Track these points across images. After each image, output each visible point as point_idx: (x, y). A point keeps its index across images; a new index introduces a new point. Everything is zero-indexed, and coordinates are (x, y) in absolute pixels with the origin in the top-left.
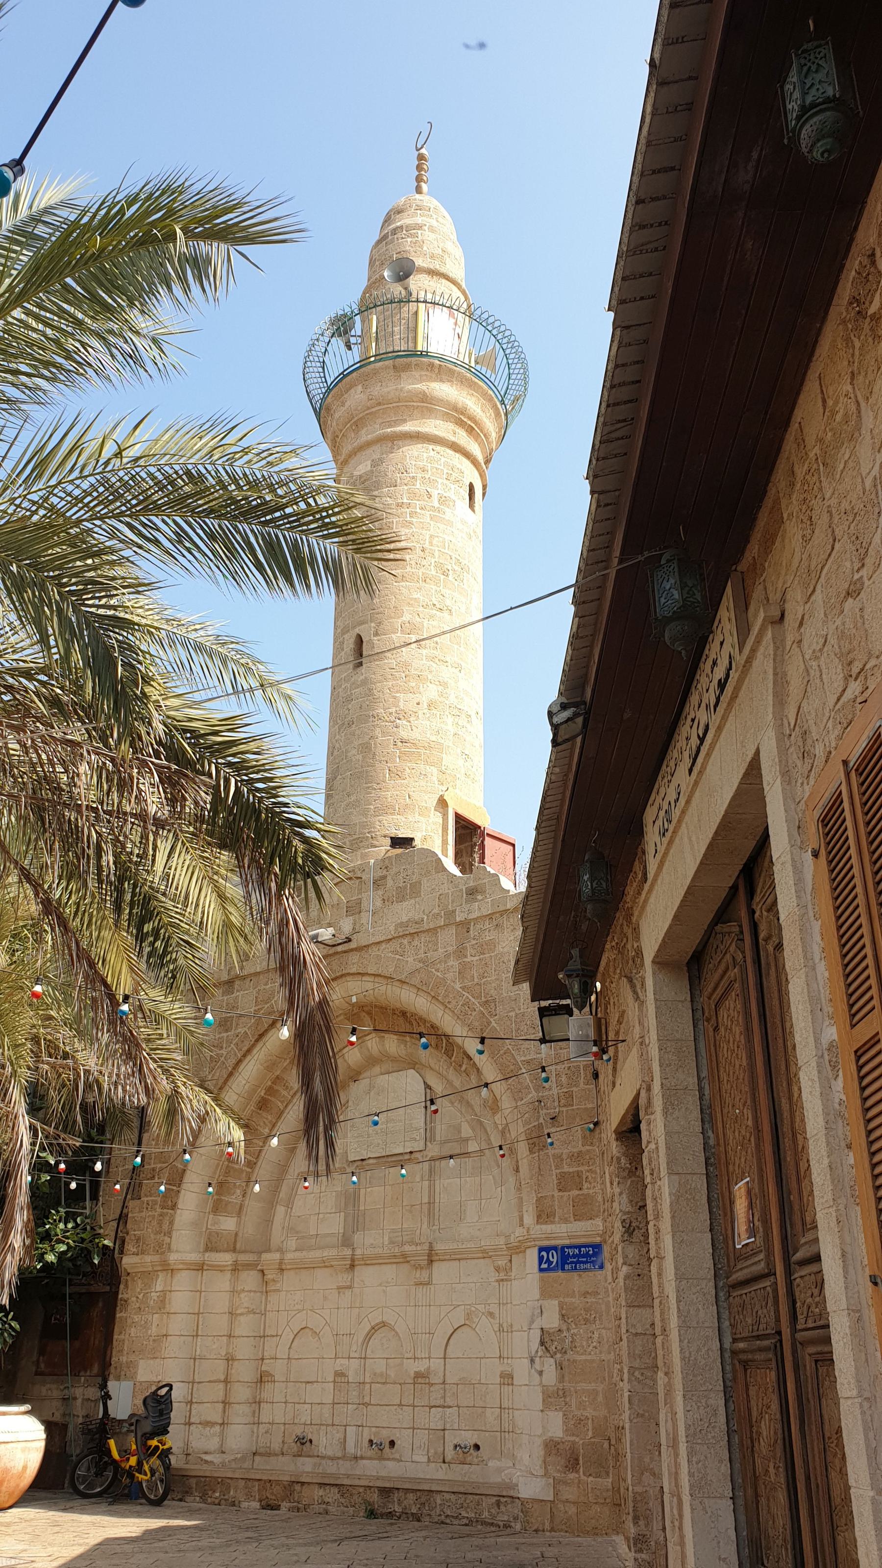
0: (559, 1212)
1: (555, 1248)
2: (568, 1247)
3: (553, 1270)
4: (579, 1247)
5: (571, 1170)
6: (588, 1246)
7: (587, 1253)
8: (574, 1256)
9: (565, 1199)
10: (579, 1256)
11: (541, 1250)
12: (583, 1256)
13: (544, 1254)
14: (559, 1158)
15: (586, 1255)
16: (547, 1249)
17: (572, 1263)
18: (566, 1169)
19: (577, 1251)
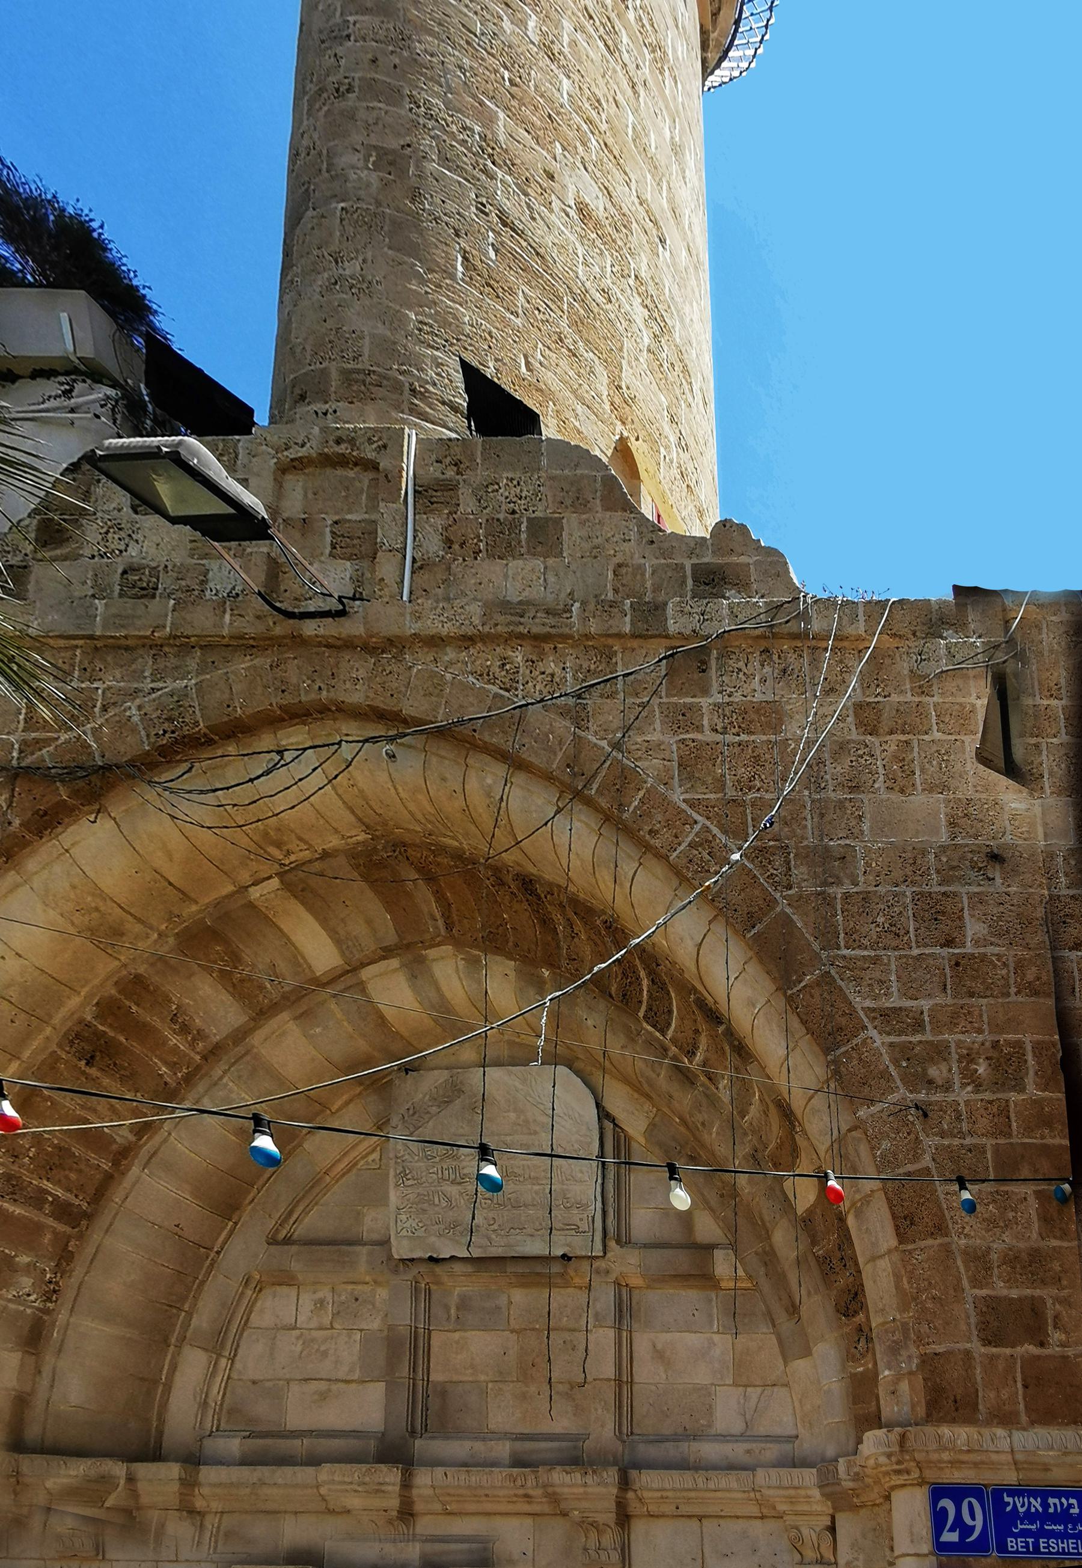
0: (987, 1399)
1: (976, 1491)
2: (1012, 1493)
3: (981, 1545)
4: (1044, 1495)
5: (1014, 1294)
6: (1068, 1495)
7: (1066, 1511)
8: (1030, 1517)
9: (1001, 1366)
10: (1045, 1517)
11: (938, 1492)
12: (1055, 1518)
13: (947, 1503)
14: (979, 1260)
15: (1064, 1516)
16: (958, 1493)
17: (1025, 1533)
18: (1001, 1289)
19: (1036, 1504)
